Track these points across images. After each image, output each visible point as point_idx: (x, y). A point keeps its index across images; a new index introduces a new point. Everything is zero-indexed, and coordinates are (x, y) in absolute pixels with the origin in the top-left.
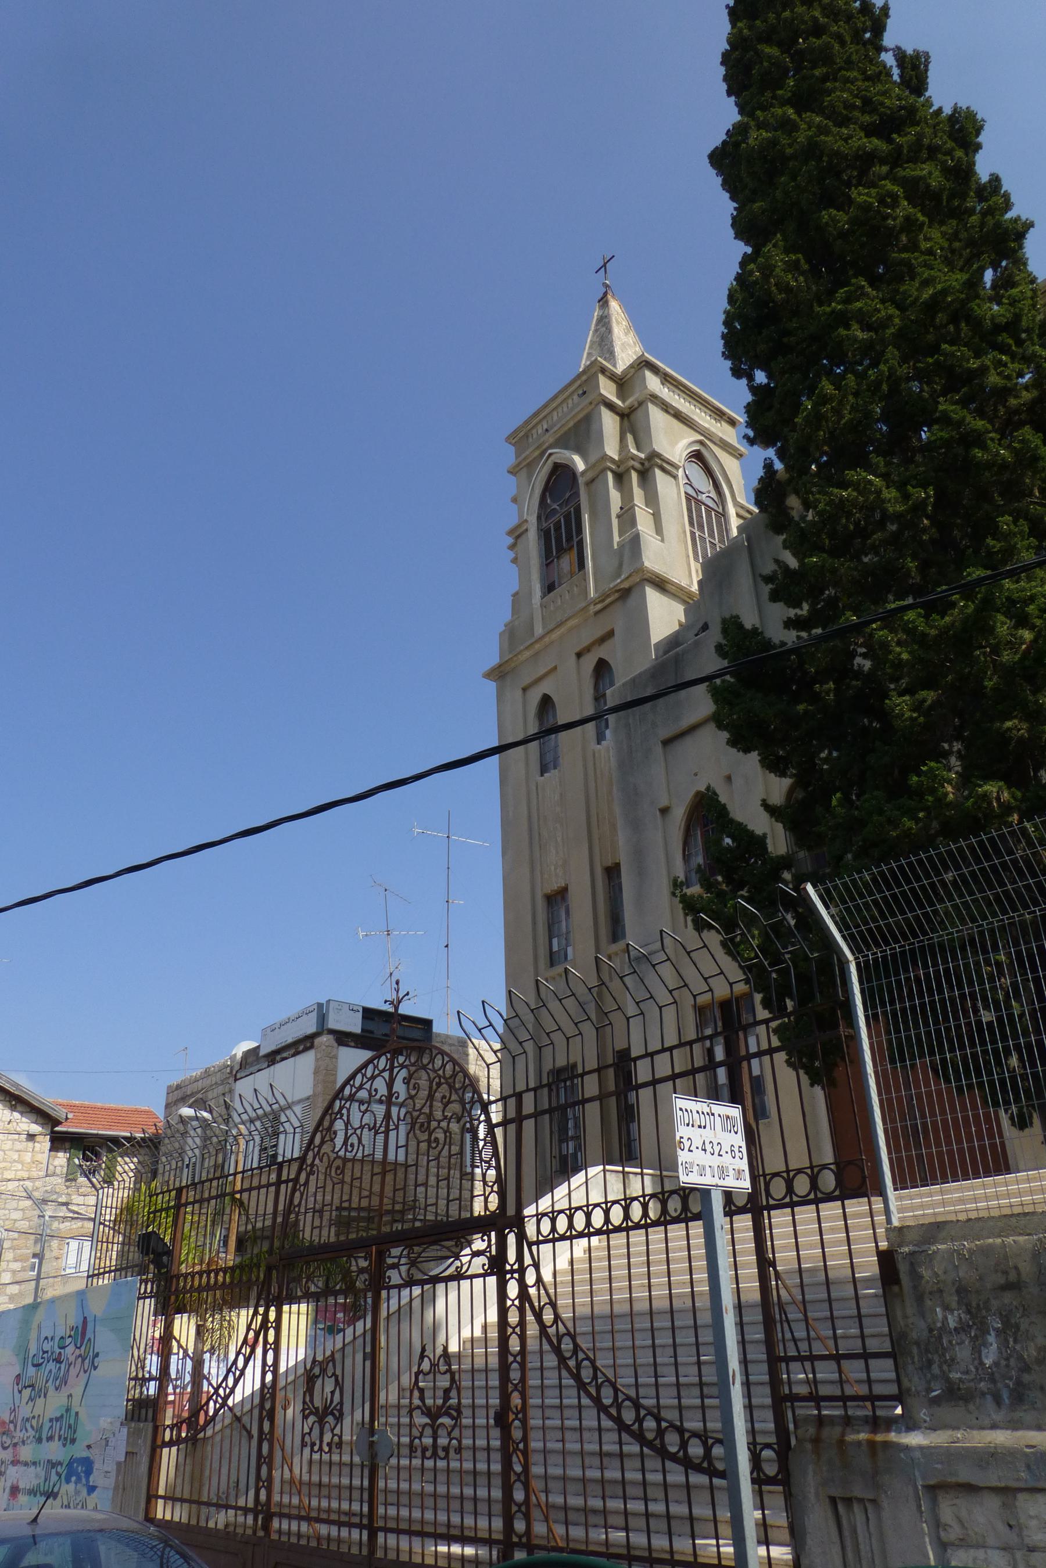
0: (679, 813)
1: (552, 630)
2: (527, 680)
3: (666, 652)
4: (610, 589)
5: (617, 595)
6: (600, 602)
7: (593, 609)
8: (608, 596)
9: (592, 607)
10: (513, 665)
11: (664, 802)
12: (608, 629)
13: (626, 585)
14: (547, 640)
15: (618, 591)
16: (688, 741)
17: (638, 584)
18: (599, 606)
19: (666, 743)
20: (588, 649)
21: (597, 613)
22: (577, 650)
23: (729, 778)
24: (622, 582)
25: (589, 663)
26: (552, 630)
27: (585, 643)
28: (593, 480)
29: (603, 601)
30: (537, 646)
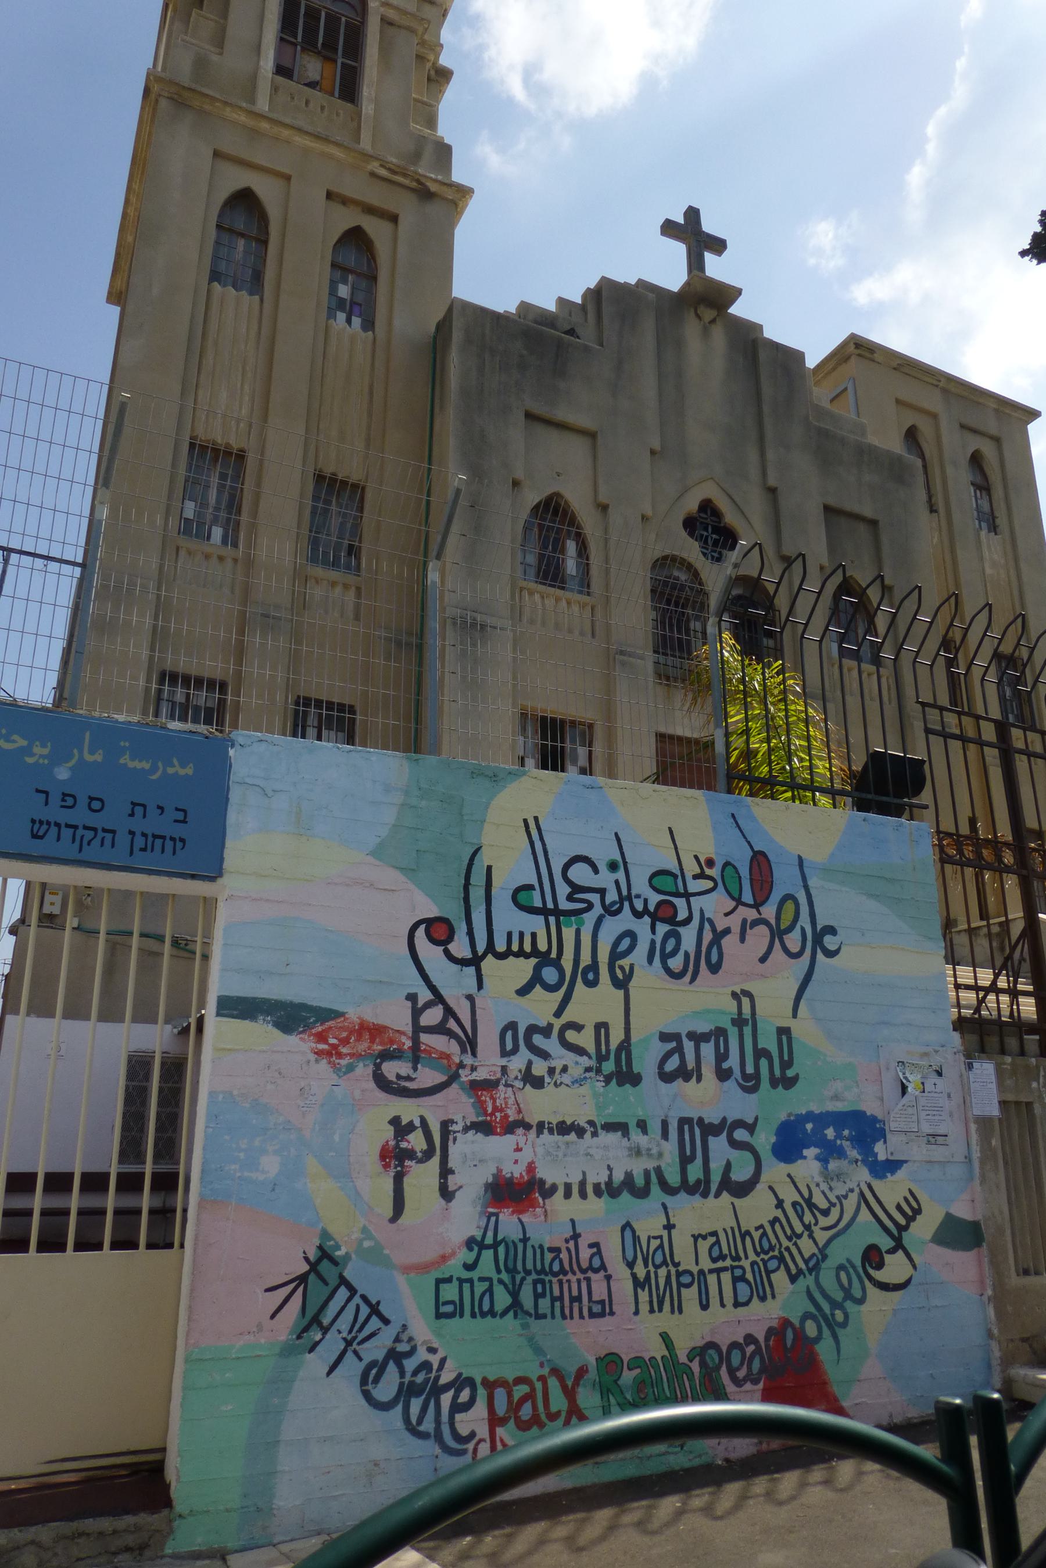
0: (532, 497)
1: (307, 133)
2: (226, 148)
3: (536, 322)
4: (416, 173)
5: (414, 184)
6: (390, 170)
7: (374, 166)
8: (405, 175)
9: (376, 164)
10: (207, 107)
11: (519, 474)
12: (390, 206)
13: (433, 187)
14: (286, 133)
15: (418, 181)
16: (554, 434)
17: (446, 199)
18: (383, 172)
19: (529, 416)
20: (345, 201)
21: (373, 174)
22: (335, 189)
23: (604, 508)
24: (436, 181)
25: (345, 219)
26: (307, 133)
27: (348, 192)
28: (391, 24)
29: (394, 173)
30: (265, 125)
